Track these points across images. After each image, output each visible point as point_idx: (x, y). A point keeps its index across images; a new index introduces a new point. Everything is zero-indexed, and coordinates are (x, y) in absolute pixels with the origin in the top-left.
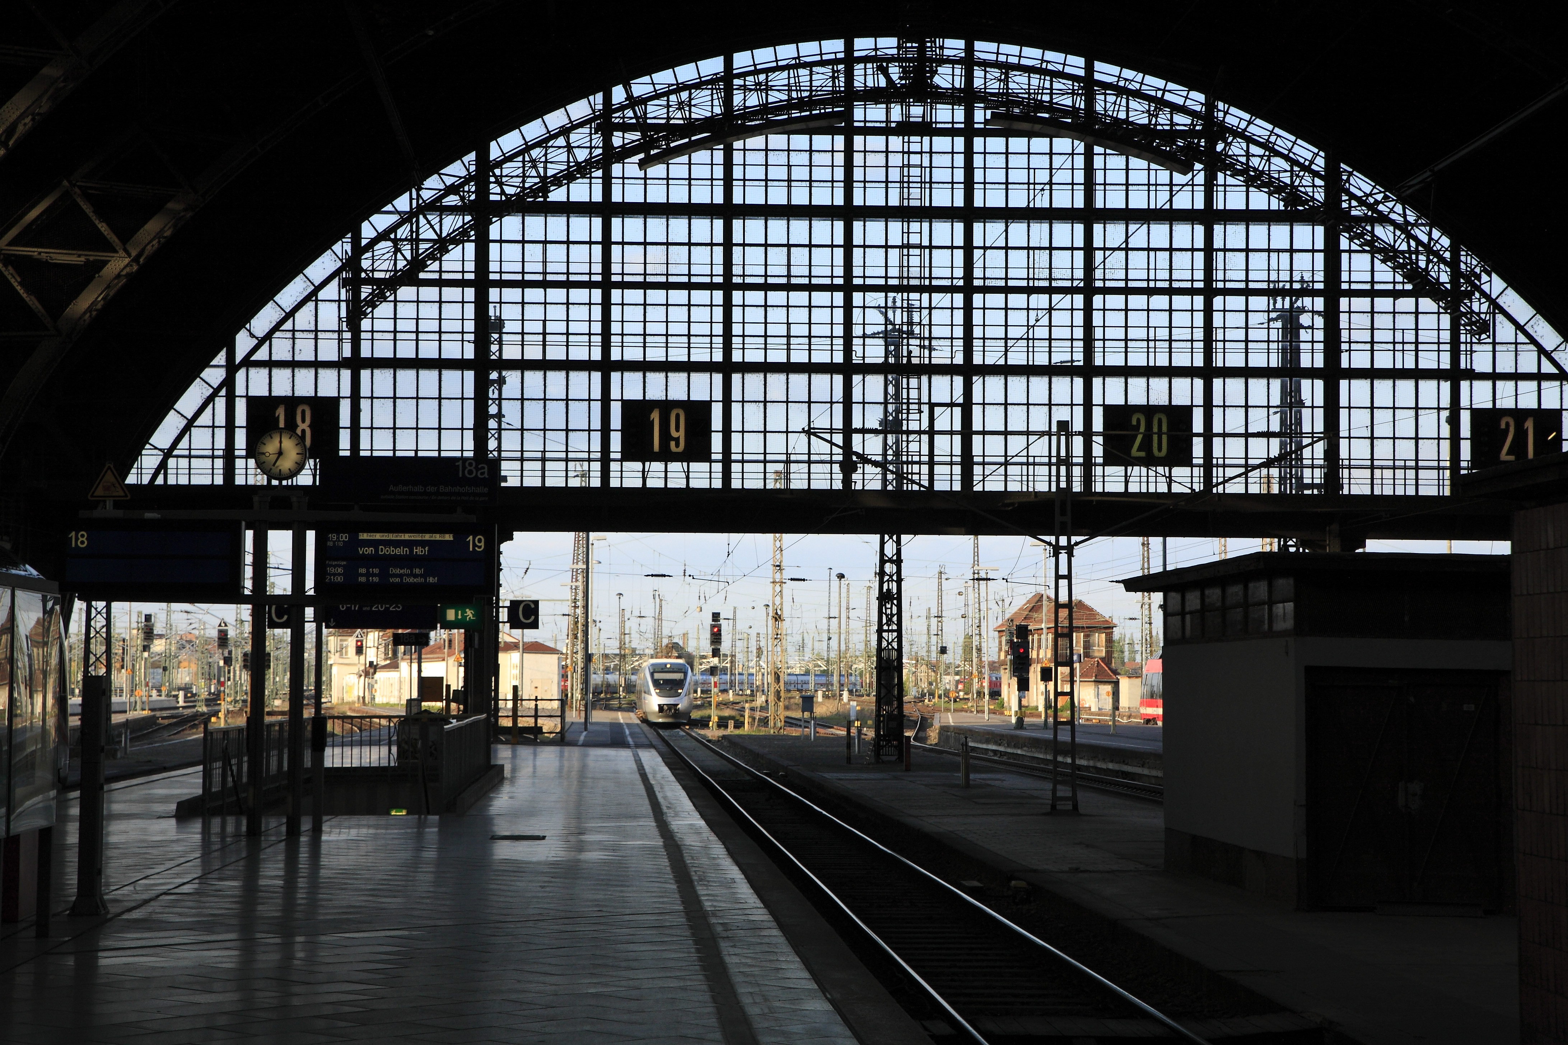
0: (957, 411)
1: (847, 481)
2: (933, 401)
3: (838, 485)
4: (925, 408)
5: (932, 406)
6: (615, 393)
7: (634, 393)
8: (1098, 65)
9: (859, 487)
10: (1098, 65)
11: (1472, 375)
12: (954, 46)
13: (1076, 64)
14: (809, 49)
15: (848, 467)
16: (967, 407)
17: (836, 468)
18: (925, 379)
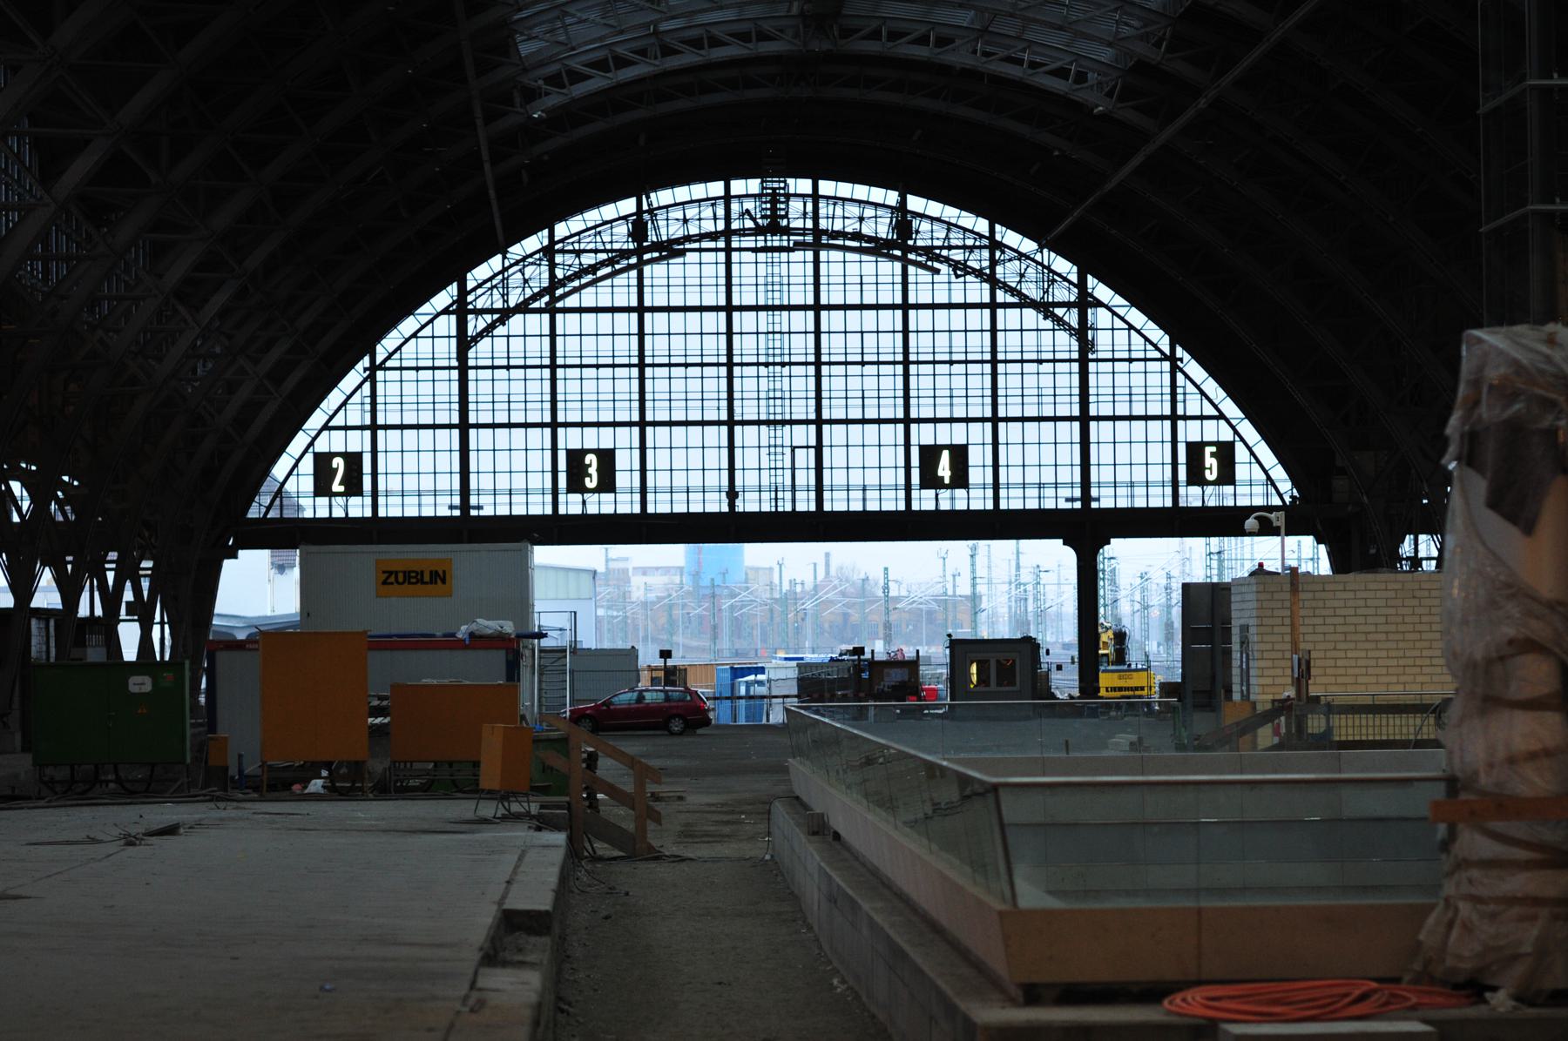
0: (812, 451)
1: (732, 505)
2: (794, 445)
3: (725, 509)
4: (788, 451)
5: (793, 449)
6: (561, 445)
7: (575, 444)
8: (910, 198)
9: (741, 510)
10: (910, 198)
11: (1185, 418)
12: (804, 186)
13: (892, 197)
14: (698, 190)
15: (732, 494)
16: (819, 448)
17: (724, 495)
18: (788, 427)
